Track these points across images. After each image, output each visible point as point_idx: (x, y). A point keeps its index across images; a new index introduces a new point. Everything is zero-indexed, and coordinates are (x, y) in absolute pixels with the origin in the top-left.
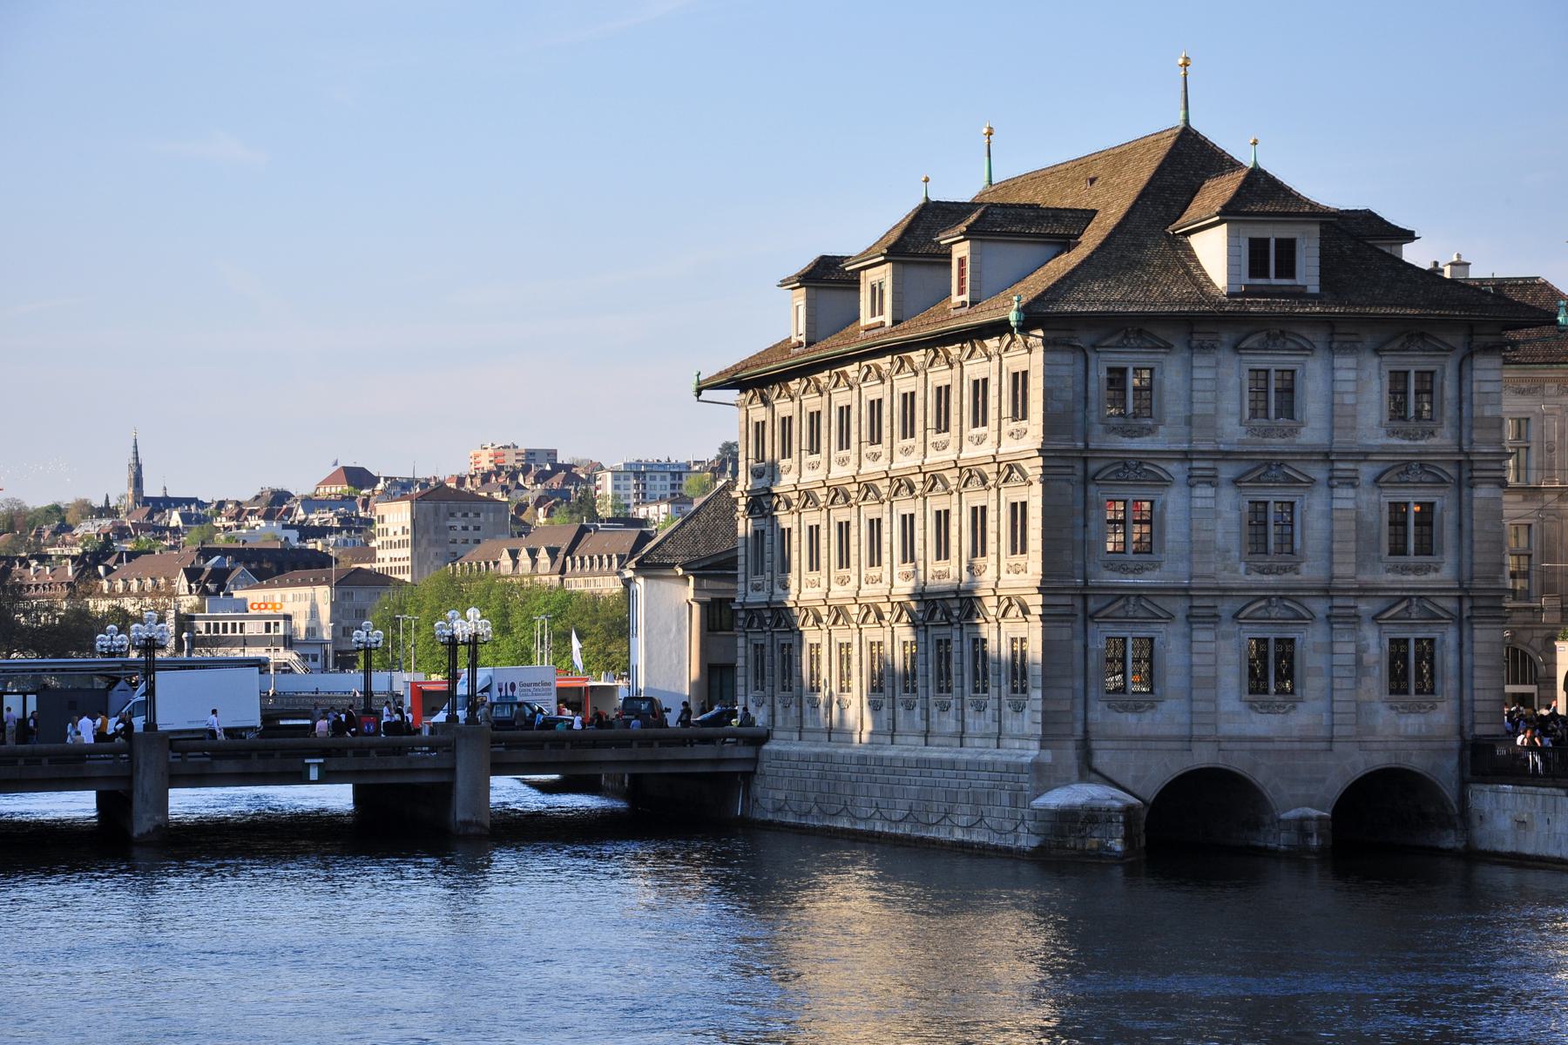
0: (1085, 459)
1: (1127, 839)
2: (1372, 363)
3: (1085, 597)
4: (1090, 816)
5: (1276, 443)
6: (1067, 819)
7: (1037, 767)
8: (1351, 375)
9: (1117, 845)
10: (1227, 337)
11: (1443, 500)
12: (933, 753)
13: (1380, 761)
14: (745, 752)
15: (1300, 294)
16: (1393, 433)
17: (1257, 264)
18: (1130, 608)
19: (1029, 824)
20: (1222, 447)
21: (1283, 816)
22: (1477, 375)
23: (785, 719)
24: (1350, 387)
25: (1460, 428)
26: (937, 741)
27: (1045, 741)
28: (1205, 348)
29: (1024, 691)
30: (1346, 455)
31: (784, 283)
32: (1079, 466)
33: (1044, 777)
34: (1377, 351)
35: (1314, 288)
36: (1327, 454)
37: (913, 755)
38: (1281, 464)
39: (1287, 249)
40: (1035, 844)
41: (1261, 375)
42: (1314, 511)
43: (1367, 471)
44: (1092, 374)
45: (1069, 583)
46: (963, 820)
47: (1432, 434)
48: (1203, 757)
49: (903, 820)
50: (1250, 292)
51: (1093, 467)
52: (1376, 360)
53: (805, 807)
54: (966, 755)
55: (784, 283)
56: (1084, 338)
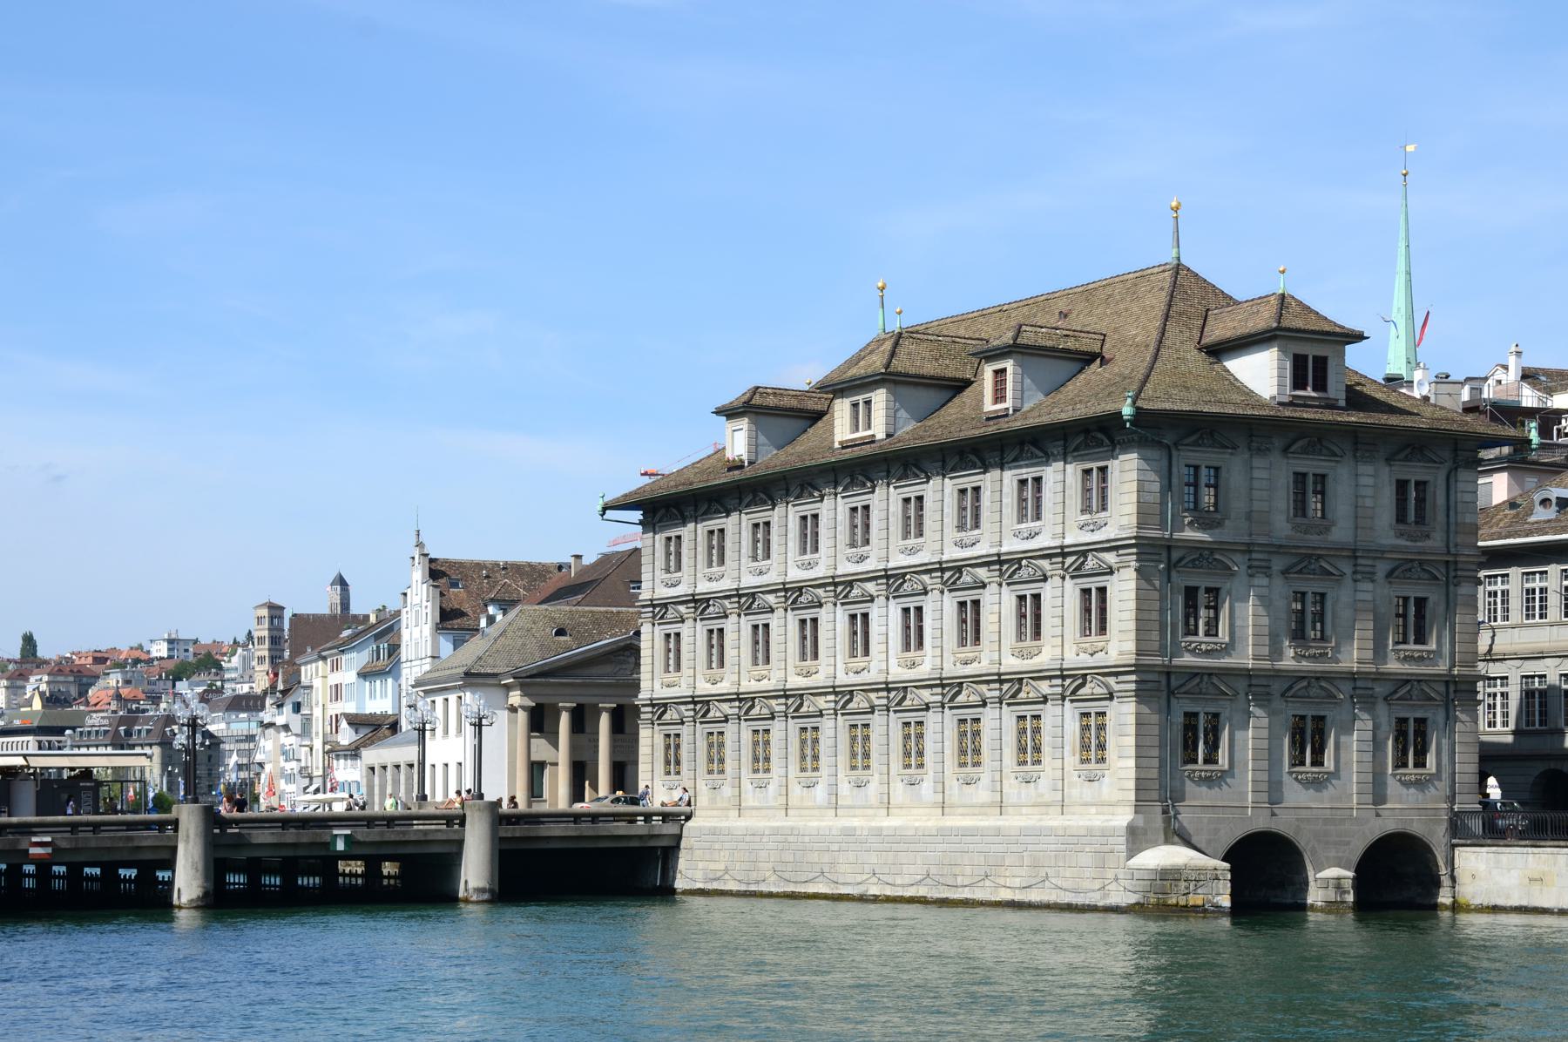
0: (1169, 548)
1: (1234, 895)
2: (1385, 471)
3: (1168, 674)
4: (1198, 878)
5: (1314, 539)
6: (1169, 876)
7: (1132, 831)
8: (1370, 481)
9: (1225, 901)
10: (1278, 443)
12: (953, 821)
13: (1390, 825)
14: (670, 829)
16: (1401, 535)
17: (1299, 383)
18: (1203, 685)
19: (1127, 883)
20: (1275, 542)
21: (1319, 875)
22: (1461, 486)
23: (713, 800)
24: (1369, 492)
25: (1448, 532)
26: (960, 810)
27: (1140, 804)
28: (1262, 451)
29: (1102, 760)
31: (718, 412)
32: (1164, 554)
33: (1136, 839)
34: (1389, 460)
35: (1342, 403)
36: (1355, 551)
37: (929, 824)
38: (1320, 557)
40: (1133, 901)
41: (1300, 478)
43: (1382, 568)
44: (1174, 470)
45: (1158, 660)
46: (1017, 882)
47: (1428, 536)
48: (1261, 823)
49: (918, 883)
51: (1175, 555)
52: (1387, 469)
53: (754, 876)
54: (1012, 822)
55: (718, 412)
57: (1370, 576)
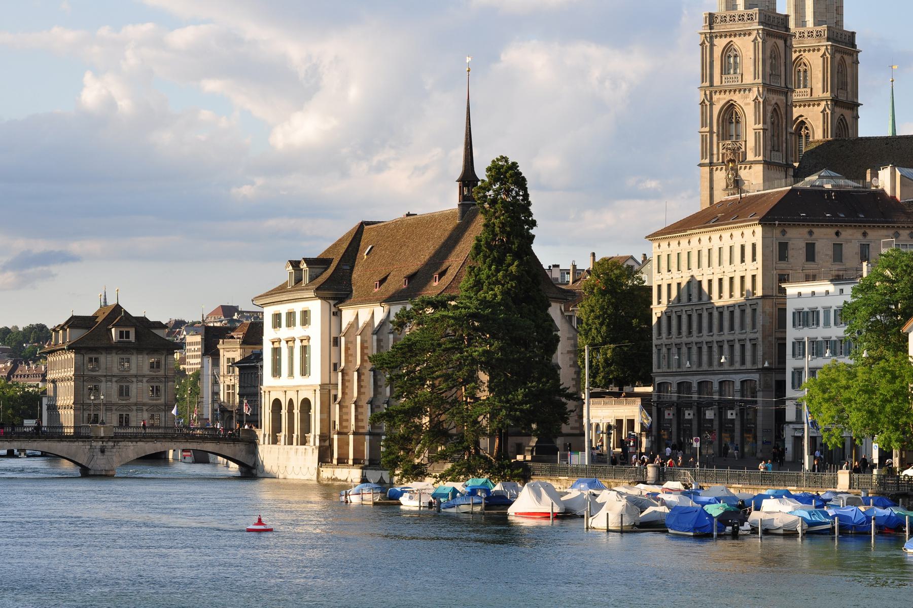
11: (162, 386)
15: (130, 342)
30: (140, 376)
39: (128, 333)
42: (134, 388)
43: (145, 380)
50: (119, 342)
56: (83, 352)
57: (142, 381)
